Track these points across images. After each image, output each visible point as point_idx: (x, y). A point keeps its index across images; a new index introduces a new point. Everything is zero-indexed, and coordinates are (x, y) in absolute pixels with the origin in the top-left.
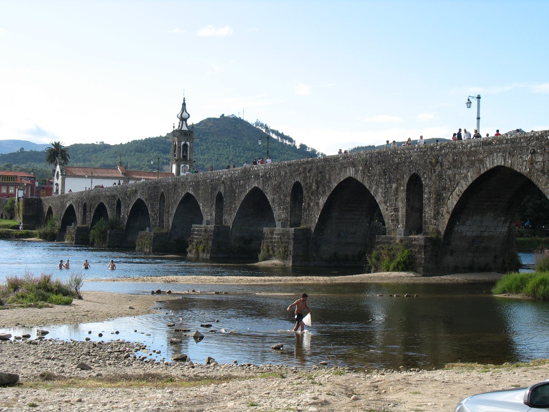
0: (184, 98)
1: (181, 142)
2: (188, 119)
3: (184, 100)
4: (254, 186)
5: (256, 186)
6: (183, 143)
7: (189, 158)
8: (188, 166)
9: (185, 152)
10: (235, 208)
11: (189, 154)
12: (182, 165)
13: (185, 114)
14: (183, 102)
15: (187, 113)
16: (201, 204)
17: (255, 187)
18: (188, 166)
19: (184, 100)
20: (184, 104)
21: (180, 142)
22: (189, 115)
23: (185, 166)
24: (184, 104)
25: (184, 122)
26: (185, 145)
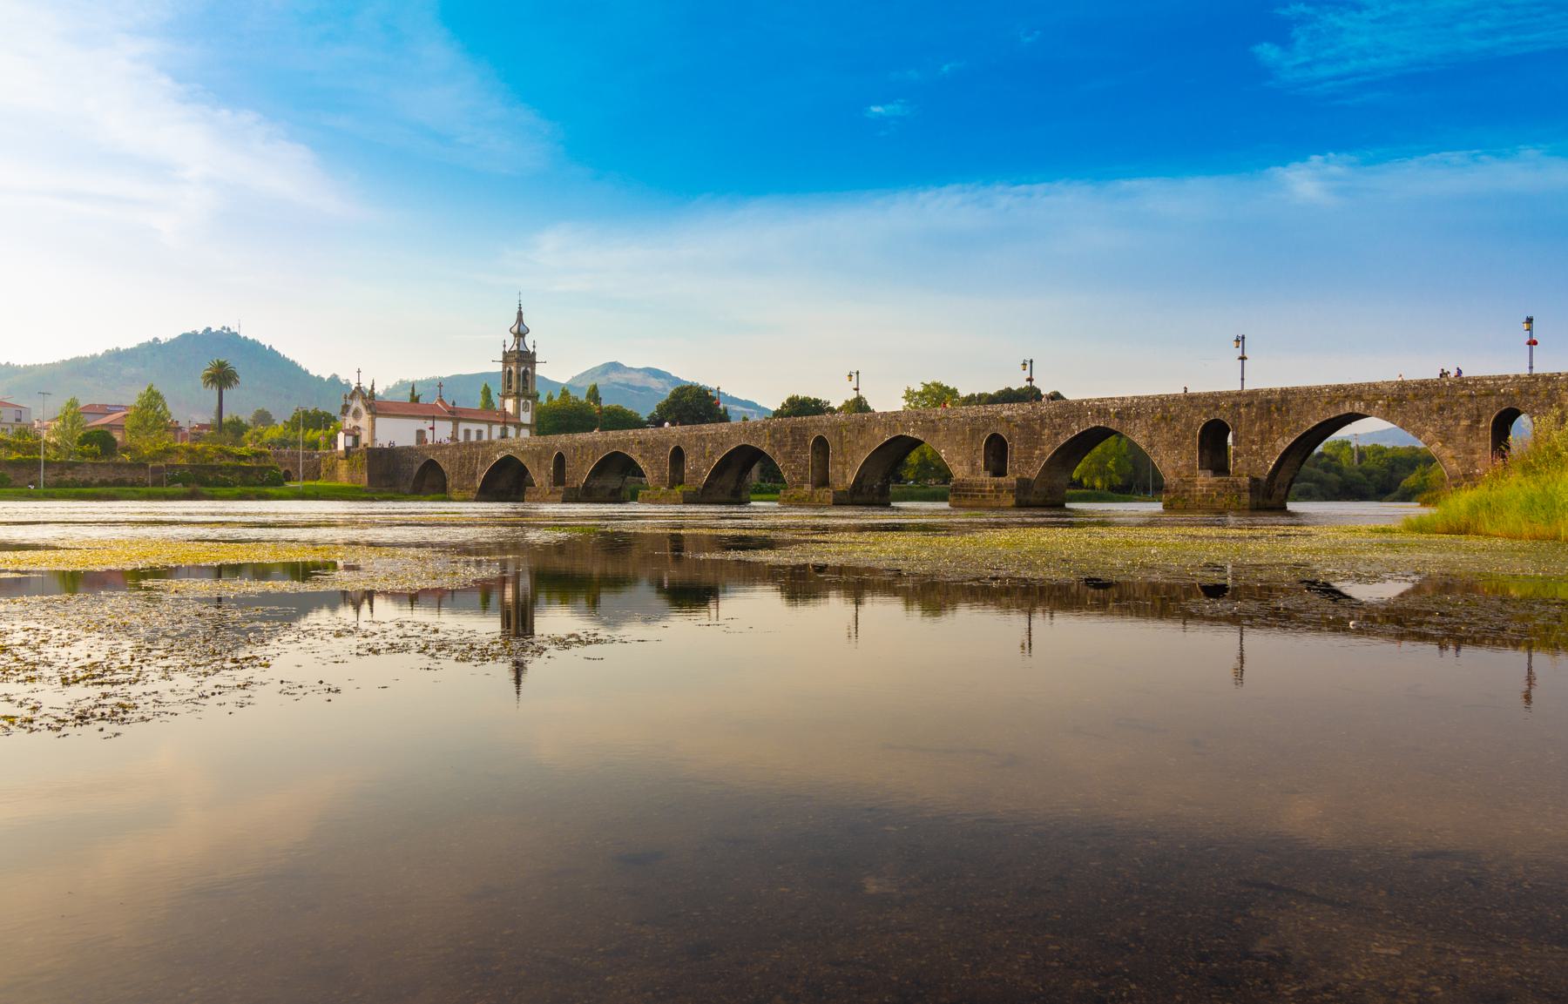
3: (520, 308)
5: (1102, 425)
6: (523, 369)
8: (529, 402)
10: (1043, 455)
12: (522, 401)
16: (943, 451)
17: (1096, 428)
19: (520, 308)
20: (520, 314)
21: (518, 368)
22: (528, 330)
23: (526, 403)
24: (520, 314)
26: (526, 372)
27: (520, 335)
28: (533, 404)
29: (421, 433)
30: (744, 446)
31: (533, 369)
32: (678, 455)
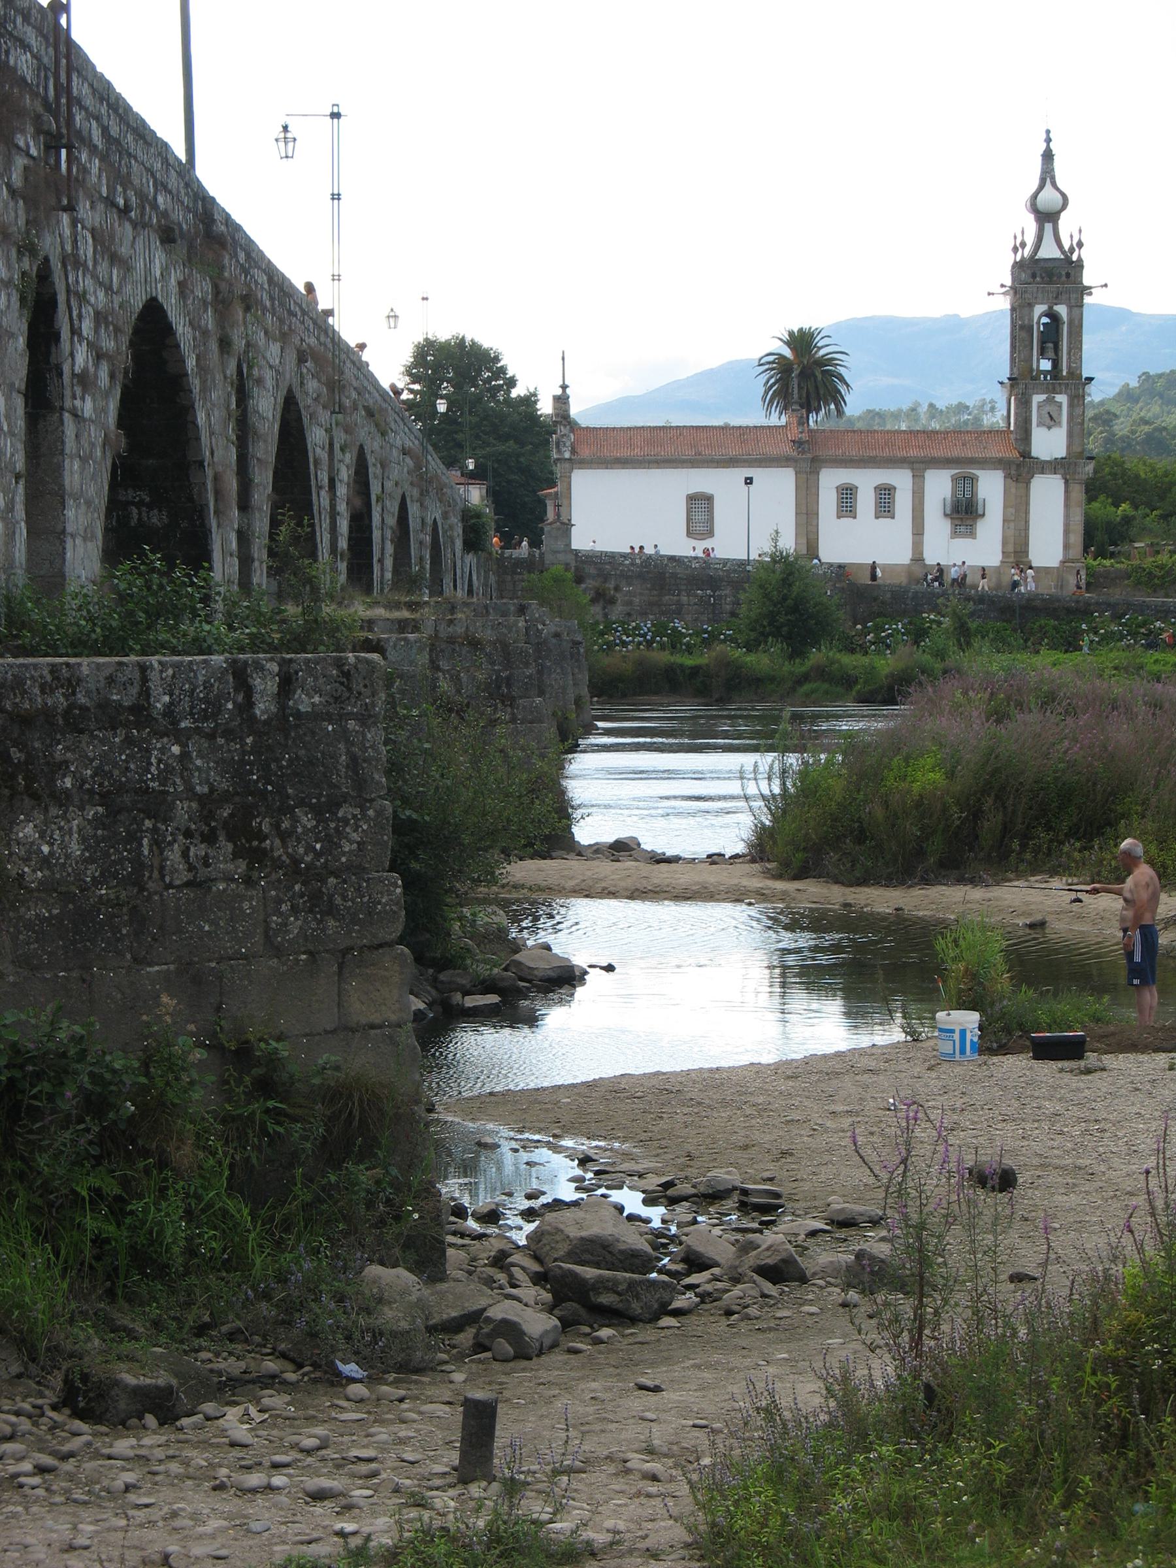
0: (1048, 132)
1: (1031, 306)
2: (1063, 215)
3: (1048, 140)
7: (1069, 367)
8: (1062, 399)
9: (1051, 345)
11: (1069, 353)
12: (1037, 399)
13: (1048, 197)
14: (1044, 145)
15: (1058, 189)
18: (1062, 399)
19: (1048, 140)
20: (1048, 156)
23: (1050, 400)
24: (1048, 156)
25: (1048, 227)
27: (1047, 217)
28: (1071, 405)
31: (1077, 305)
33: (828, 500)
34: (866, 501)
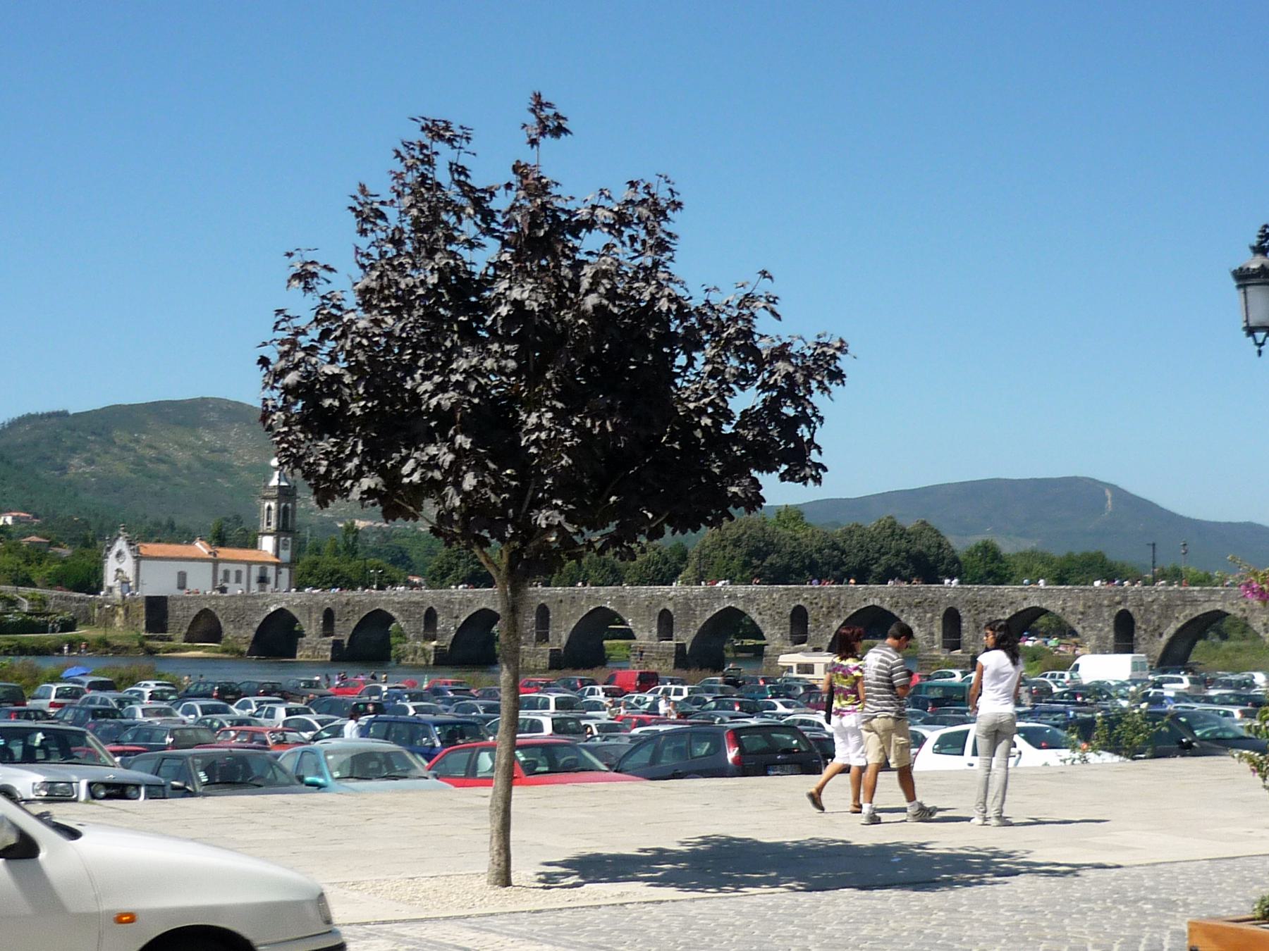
4: (727, 605)
6: (283, 505)
21: (279, 504)
26: (286, 508)
28: (293, 542)
29: (182, 577)
30: (484, 610)
31: (294, 504)
32: (431, 617)
33: (220, 576)
34: (232, 577)
